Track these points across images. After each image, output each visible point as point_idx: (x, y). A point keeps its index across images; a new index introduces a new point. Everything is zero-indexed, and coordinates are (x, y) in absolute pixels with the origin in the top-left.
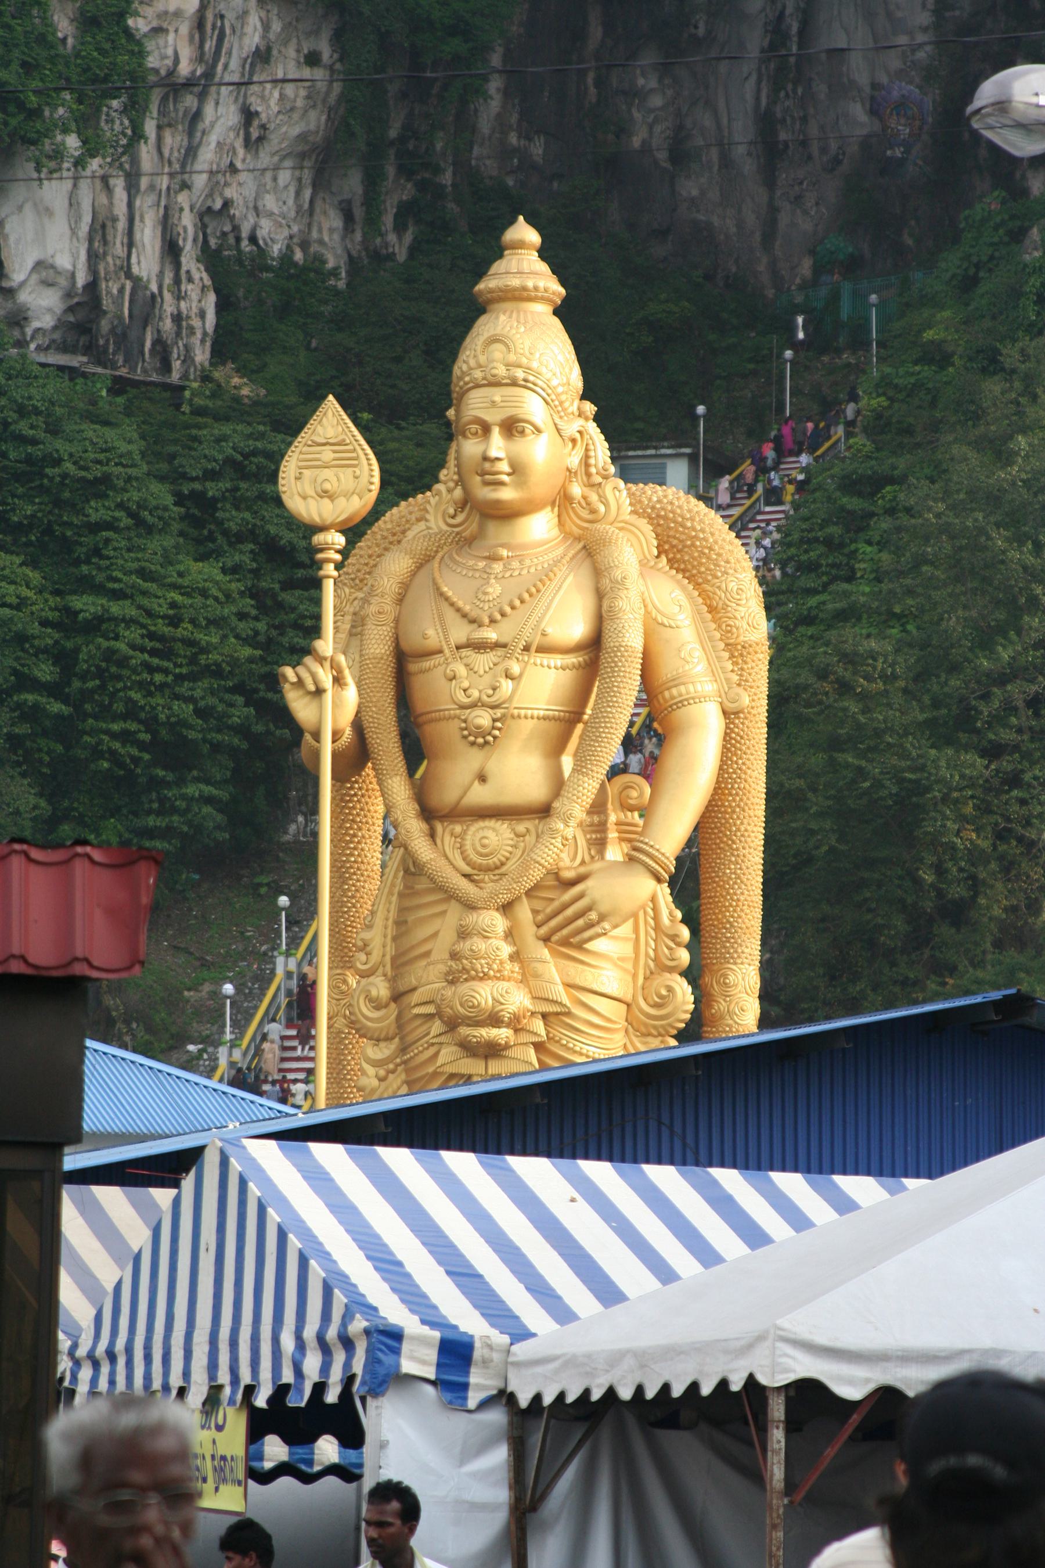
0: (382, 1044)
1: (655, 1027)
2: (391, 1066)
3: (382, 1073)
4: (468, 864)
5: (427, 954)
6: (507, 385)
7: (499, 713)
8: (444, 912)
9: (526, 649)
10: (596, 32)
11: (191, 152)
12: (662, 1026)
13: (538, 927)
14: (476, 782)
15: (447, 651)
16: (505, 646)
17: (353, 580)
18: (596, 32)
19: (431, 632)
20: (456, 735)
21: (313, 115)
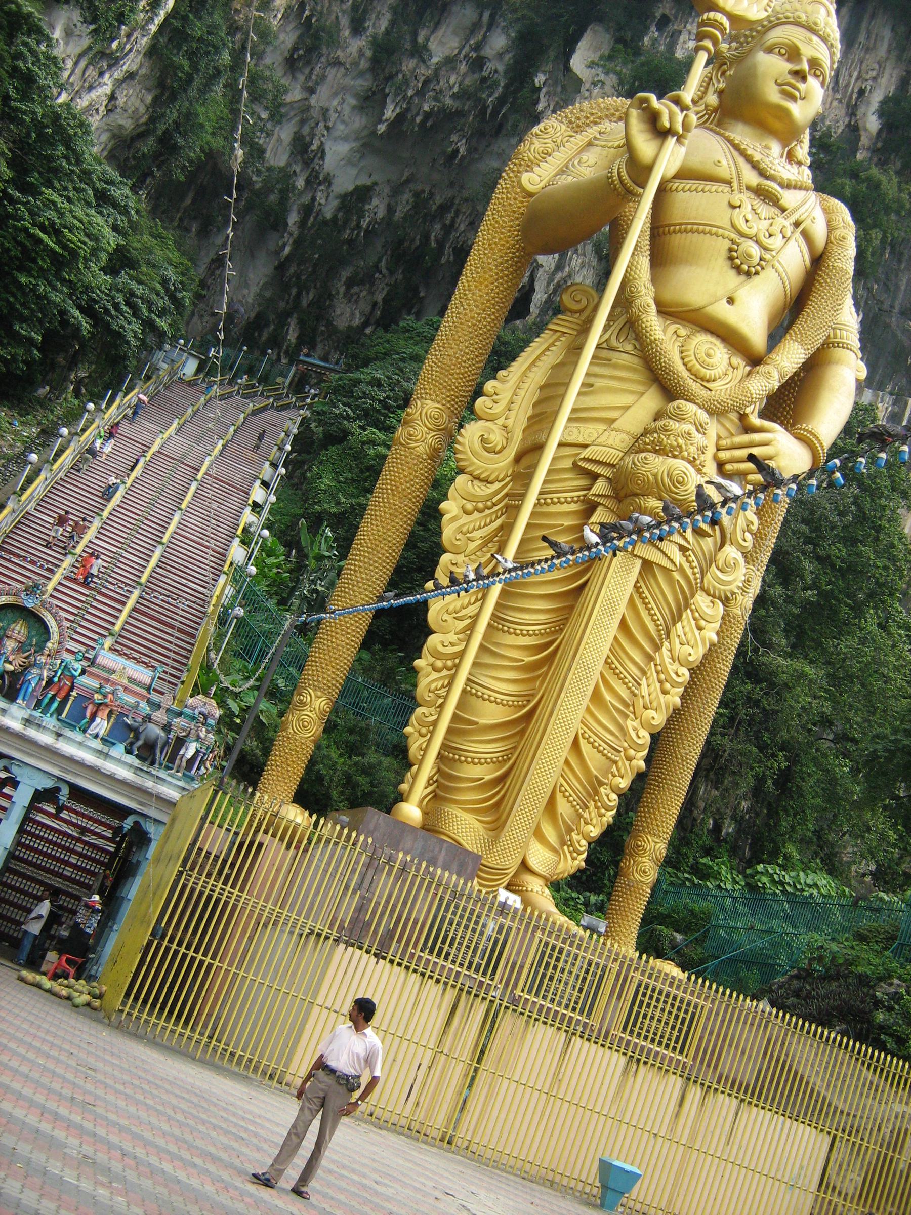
0: (476, 482)
1: (714, 587)
2: (480, 505)
3: (469, 506)
4: (685, 365)
5: (613, 421)
6: (820, 37)
7: (767, 256)
8: (642, 394)
9: (797, 224)
10: (188, 201)
11: (91, 88)
12: (719, 590)
13: (718, 450)
14: (724, 301)
15: (735, 185)
16: (783, 210)
17: (571, 122)
18: (188, 201)
19: (724, 162)
20: (724, 253)
21: (130, 121)
